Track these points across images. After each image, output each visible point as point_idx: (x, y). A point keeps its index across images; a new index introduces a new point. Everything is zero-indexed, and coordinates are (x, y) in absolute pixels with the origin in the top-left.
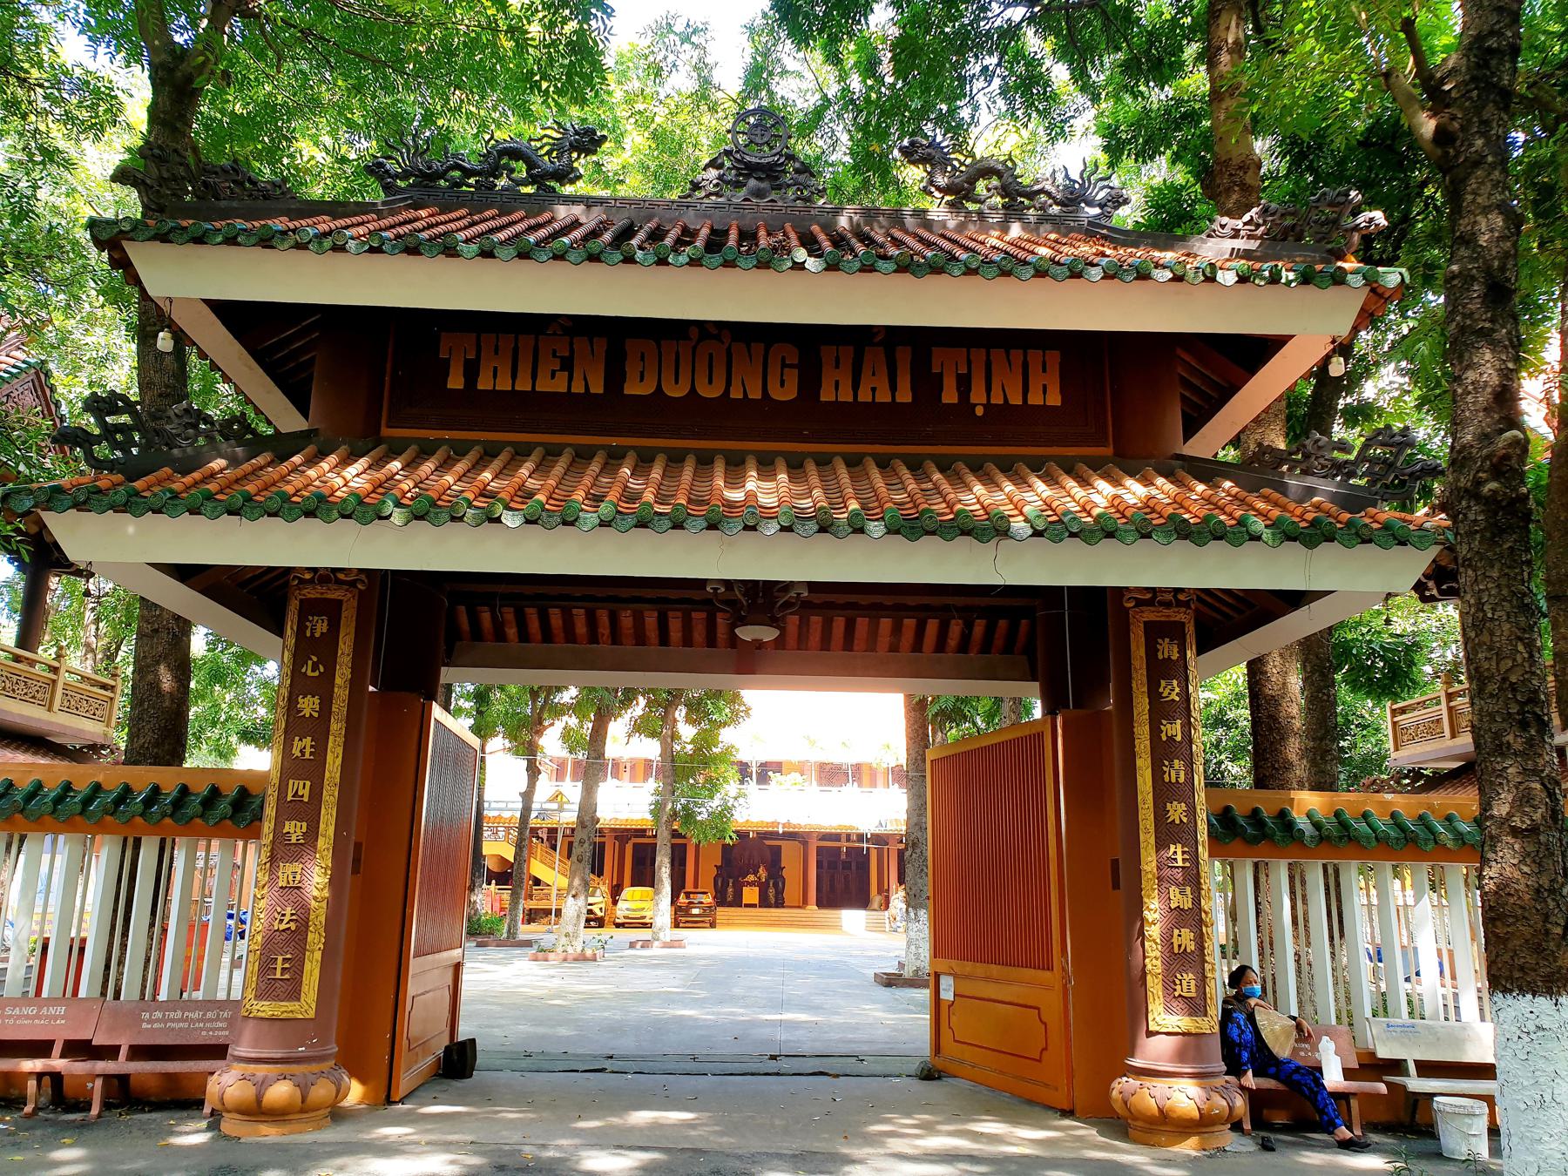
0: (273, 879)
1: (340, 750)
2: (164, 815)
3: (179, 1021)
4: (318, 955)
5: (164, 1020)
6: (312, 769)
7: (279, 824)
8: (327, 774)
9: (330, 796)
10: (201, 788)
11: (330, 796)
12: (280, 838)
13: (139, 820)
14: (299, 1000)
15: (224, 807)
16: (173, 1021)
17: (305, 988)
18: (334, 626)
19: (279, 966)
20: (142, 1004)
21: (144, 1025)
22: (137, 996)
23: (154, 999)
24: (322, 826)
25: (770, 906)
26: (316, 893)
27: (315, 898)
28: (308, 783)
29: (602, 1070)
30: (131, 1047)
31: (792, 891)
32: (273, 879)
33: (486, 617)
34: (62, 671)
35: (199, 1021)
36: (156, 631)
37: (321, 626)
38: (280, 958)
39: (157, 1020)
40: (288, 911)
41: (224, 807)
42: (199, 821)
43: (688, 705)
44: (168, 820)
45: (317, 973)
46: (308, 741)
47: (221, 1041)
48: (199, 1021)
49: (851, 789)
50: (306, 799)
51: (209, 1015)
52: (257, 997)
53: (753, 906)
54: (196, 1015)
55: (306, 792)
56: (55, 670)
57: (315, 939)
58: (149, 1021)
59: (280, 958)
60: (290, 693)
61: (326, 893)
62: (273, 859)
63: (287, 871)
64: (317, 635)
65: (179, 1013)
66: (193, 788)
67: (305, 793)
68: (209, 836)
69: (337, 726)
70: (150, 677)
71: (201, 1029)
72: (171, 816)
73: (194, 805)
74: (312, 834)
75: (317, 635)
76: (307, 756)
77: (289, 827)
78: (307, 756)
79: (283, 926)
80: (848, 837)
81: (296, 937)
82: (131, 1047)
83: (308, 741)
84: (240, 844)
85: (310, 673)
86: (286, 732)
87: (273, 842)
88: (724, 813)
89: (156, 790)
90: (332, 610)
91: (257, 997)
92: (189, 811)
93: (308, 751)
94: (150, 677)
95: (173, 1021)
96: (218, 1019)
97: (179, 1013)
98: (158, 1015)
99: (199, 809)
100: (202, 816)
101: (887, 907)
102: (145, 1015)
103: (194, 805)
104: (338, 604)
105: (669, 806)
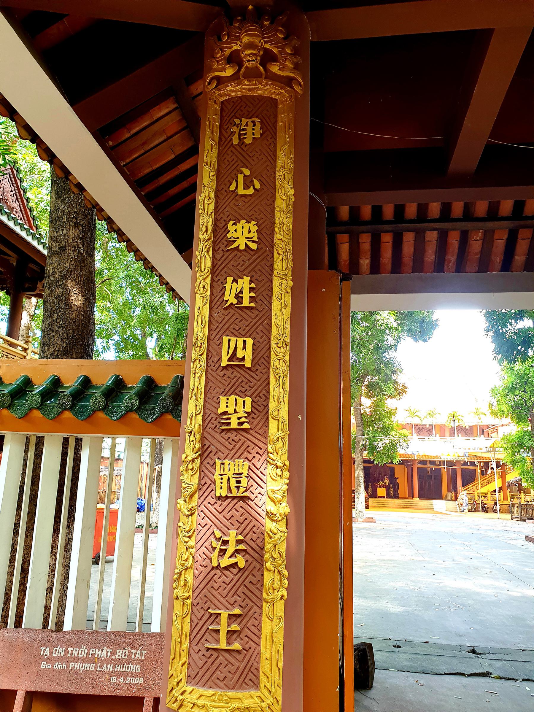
0: (205, 486)
1: (288, 298)
2: (64, 409)
3: (84, 660)
4: (280, 608)
5: (67, 659)
6: (253, 319)
7: (210, 399)
8: (274, 330)
9: (280, 360)
10: (103, 380)
11: (280, 360)
12: (215, 422)
13: (37, 414)
14: (256, 686)
15: (129, 398)
16: (77, 660)
17: (265, 666)
18: (270, 131)
19: (223, 626)
20: (44, 634)
21: (44, 665)
22: (39, 624)
23: (59, 625)
24: (273, 404)
25: (391, 497)
26: (271, 507)
27: (270, 515)
28: (250, 342)
29: (486, 675)
30: (28, 693)
31: (403, 488)
32: (205, 486)
33: (344, 249)
34: (30, 351)
35: (108, 661)
36: (63, 249)
37: (252, 131)
38: (224, 614)
39: (60, 659)
40: (232, 536)
41: (129, 398)
42: (101, 415)
43: (370, 386)
44: (68, 415)
45: (280, 637)
46: (245, 283)
47: (134, 693)
48: (108, 661)
49: (436, 439)
50: (248, 363)
51: (120, 654)
52: (189, 679)
53: (383, 497)
54: (103, 653)
55: (248, 353)
56: (25, 350)
57: (276, 584)
58: (50, 660)
59: (224, 614)
60: (215, 220)
61: (284, 508)
62: (204, 452)
63: (227, 470)
64: (248, 141)
65: (83, 652)
66: (95, 381)
67: (247, 354)
68: (113, 432)
69: (281, 264)
70: (59, 291)
71: (111, 674)
72: (72, 408)
73: (96, 398)
74: (260, 412)
75: (248, 141)
76: (246, 303)
77: (226, 404)
78: (246, 303)
79: (225, 562)
80: (433, 463)
81: (246, 579)
82: (28, 693)
83: (245, 283)
84: (146, 443)
85: (241, 191)
86: (213, 272)
87: (203, 428)
88: (392, 447)
89: (56, 383)
90: (264, 110)
91: (189, 679)
92: (91, 403)
93: (246, 295)
94: (59, 291)
95: (77, 660)
96: (129, 661)
97: (84, 649)
98: (60, 651)
99: (102, 401)
100: (105, 408)
101: (456, 499)
102: (45, 651)
103: (96, 398)
104: (274, 103)
105: (361, 443)
